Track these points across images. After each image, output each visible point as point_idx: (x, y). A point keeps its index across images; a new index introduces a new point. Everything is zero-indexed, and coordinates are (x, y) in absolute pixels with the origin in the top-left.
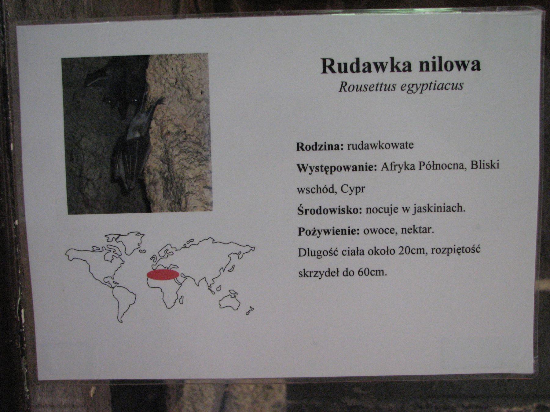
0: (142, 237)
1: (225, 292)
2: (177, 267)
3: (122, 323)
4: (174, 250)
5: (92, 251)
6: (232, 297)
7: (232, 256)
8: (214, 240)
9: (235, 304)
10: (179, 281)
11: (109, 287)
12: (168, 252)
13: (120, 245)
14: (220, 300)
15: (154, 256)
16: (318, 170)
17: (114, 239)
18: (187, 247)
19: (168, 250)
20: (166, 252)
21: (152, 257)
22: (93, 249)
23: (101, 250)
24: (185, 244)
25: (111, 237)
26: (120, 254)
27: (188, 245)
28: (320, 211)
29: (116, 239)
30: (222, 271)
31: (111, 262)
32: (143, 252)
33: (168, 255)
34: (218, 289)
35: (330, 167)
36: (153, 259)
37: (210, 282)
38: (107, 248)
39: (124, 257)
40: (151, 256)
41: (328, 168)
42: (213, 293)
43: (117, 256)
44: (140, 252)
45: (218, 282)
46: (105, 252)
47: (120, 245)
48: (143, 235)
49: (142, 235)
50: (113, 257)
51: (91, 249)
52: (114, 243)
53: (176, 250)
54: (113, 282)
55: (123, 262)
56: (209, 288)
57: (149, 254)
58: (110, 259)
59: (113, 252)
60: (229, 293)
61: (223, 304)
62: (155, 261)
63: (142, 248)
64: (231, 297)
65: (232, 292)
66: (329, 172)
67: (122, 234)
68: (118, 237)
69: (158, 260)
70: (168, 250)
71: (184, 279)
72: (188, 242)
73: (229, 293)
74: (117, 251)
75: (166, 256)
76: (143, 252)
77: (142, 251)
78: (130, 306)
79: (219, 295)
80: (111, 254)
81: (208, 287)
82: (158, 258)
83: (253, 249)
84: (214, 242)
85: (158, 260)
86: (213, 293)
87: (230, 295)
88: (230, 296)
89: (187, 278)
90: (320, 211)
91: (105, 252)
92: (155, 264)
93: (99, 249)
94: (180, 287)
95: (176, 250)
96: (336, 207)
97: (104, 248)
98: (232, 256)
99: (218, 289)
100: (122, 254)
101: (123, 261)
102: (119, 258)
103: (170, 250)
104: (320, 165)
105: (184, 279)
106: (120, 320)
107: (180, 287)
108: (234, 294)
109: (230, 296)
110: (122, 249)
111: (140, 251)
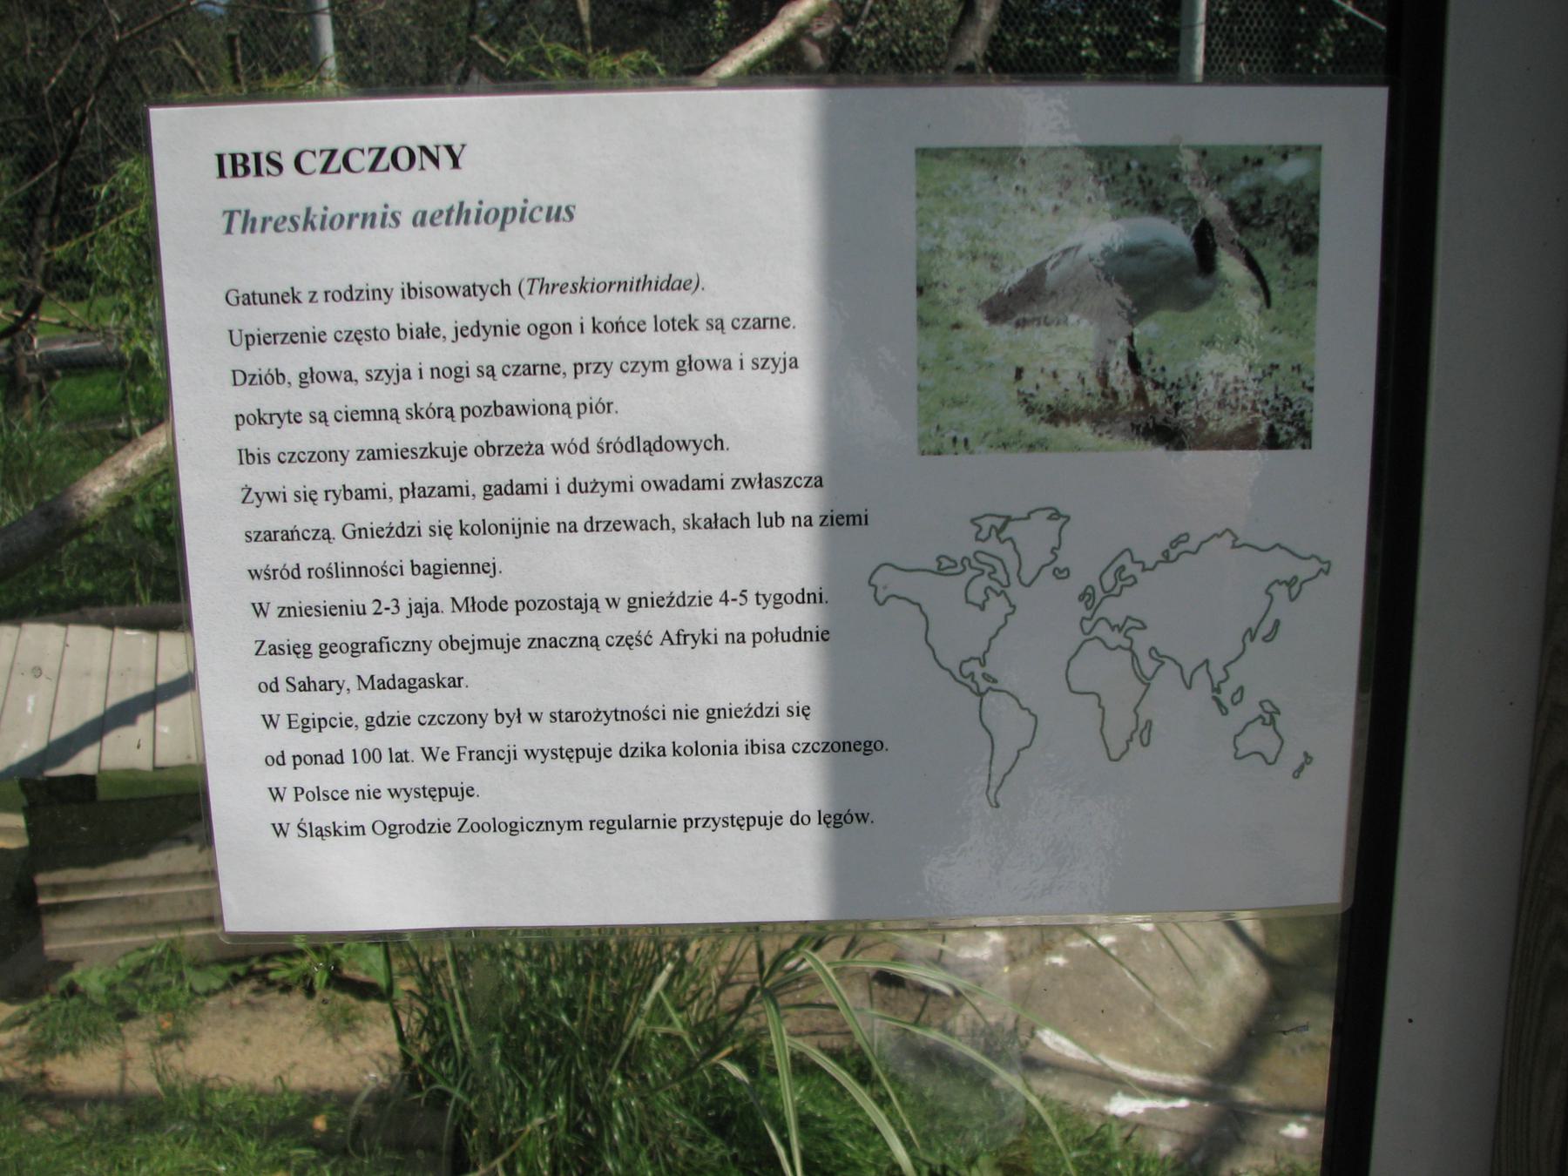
1: (1249, 709)
5: (935, 569)
9: (1269, 744)
13: (1006, 551)
14: (1238, 731)
15: (1090, 591)
22: (940, 563)
23: (960, 568)
26: (1005, 583)
31: (982, 607)
32: (1062, 574)
34: (1237, 698)
37: (1218, 675)
38: (974, 563)
39: (1015, 591)
43: (998, 588)
46: (970, 573)
47: (1006, 551)
52: (992, 546)
57: (1075, 585)
58: (979, 599)
60: (1259, 711)
61: (1246, 744)
62: (1089, 604)
65: (1268, 707)
73: (1259, 711)
74: (1000, 575)
75: (1116, 591)
76: (1062, 574)
79: (1239, 715)
80: (984, 581)
82: (1099, 594)
86: (1224, 710)
87: (1261, 717)
89: (1163, 663)
91: (970, 573)
97: (966, 562)
101: (1011, 605)
102: (1002, 596)
108: (1271, 714)
110: (1012, 565)
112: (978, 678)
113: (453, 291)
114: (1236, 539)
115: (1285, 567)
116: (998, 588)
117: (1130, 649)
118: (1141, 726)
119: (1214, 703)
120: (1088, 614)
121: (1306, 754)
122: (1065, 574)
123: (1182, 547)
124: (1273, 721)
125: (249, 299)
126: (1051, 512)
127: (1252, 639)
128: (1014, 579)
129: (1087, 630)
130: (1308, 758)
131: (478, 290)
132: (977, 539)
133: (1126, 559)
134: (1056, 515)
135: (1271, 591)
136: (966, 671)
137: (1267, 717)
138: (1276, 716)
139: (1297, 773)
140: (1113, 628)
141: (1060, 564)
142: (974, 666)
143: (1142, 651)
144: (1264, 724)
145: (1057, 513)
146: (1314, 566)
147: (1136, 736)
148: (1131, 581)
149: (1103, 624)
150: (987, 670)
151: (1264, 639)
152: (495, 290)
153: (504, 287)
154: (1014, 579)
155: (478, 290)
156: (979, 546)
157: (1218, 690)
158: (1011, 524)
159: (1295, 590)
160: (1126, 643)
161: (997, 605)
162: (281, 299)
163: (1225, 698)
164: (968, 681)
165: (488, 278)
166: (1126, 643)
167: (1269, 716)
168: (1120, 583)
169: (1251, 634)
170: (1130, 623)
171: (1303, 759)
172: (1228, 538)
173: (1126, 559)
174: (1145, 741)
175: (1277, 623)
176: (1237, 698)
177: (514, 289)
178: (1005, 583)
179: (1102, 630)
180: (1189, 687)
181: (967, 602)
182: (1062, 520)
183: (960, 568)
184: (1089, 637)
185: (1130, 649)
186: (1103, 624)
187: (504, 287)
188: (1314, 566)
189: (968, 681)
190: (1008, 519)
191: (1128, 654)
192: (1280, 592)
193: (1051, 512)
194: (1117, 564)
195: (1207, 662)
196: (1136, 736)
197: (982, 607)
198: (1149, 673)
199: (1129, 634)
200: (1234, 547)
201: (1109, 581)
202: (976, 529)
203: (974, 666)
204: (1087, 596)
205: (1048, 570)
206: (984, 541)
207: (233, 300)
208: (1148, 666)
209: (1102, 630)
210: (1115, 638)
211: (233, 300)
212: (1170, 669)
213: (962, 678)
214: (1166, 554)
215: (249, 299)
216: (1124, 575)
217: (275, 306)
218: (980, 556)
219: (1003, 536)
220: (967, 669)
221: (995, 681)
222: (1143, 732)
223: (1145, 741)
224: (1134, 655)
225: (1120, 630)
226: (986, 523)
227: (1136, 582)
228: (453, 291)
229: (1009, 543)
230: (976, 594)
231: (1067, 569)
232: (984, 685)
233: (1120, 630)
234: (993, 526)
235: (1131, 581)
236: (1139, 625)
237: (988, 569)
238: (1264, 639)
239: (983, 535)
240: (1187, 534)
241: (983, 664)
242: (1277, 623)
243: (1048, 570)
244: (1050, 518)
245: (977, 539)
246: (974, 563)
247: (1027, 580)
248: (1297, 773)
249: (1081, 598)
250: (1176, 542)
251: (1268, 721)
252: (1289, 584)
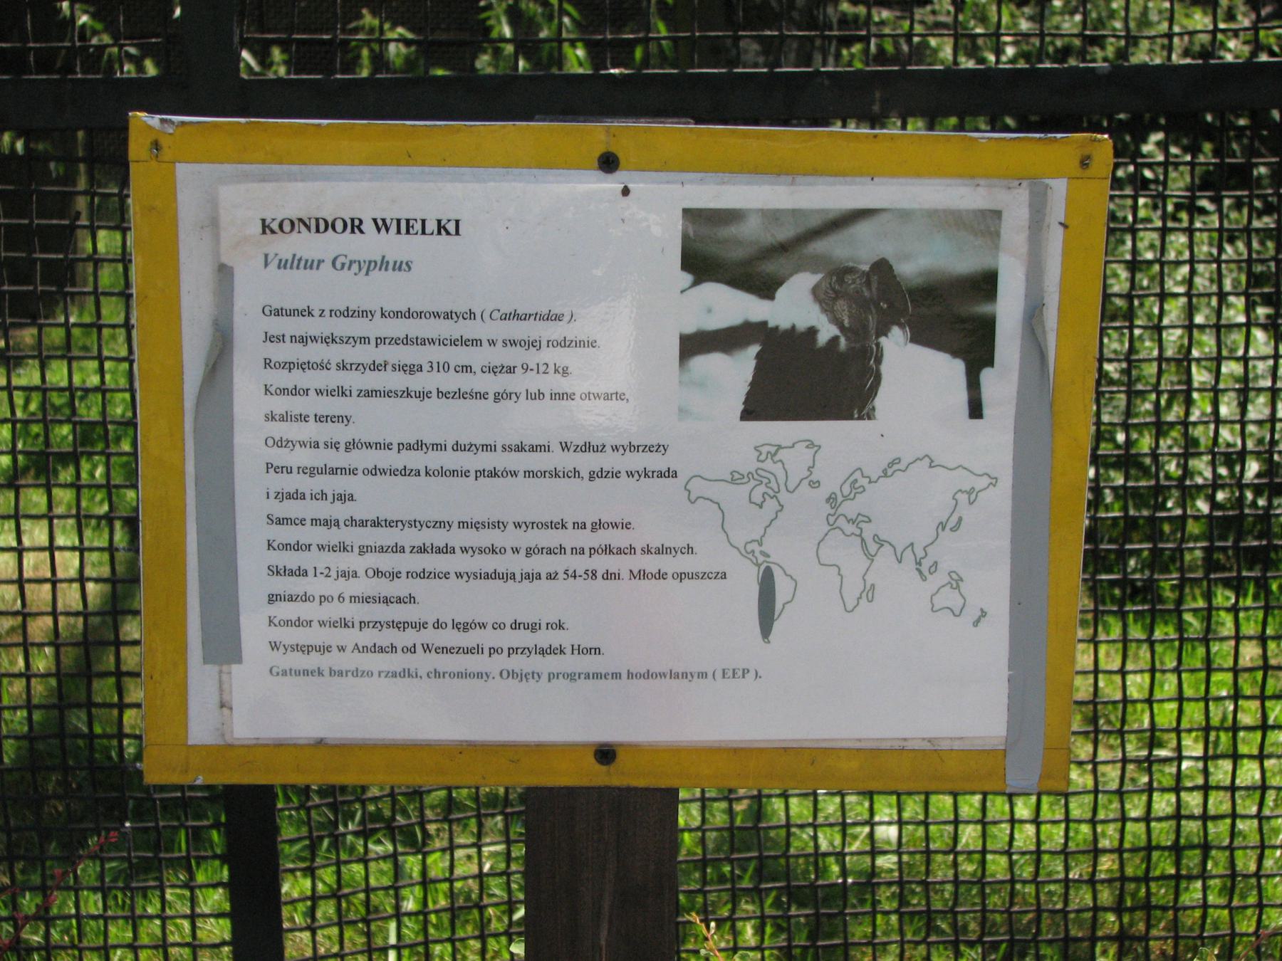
1: (940, 578)
9: (956, 602)
13: (777, 469)
31: (761, 507)
32: (815, 484)
34: (933, 569)
37: (920, 554)
38: (756, 476)
39: (783, 496)
40: (827, 496)
43: (772, 493)
46: (753, 483)
52: (768, 465)
57: (824, 492)
60: (947, 579)
61: (939, 601)
65: (954, 576)
68: (775, 454)
73: (947, 579)
74: (774, 485)
75: (852, 496)
76: (815, 484)
80: (762, 489)
82: (840, 499)
89: (882, 545)
91: (753, 483)
110: (782, 481)
112: (757, 554)
113: (436, 315)
114: (932, 461)
115: (967, 482)
116: (772, 493)
117: (860, 535)
118: (868, 587)
119: (917, 573)
120: (832, 512)
121: (982, 610)
123: (896, 467)
124: (958, 587)
125: (278, 312)
126: (808, 443)
127: (943, 529)
128: (783, 488)
129: (831, 522)
130: (984, 613)
131: (454, 315)
132: (758, 461)
133: (858, 475)
134: (811, 444)
135: (957, 497)
136: (749, 550)
138: (960, 583)
139: (976, 623)
140: (848, 522)
141: (814, 478)
143: (868, 535)
144: (952, 587)
145: (813, 444)
146: (985, 481)
147: (864, 595)
148: (861, 489)
149: (842, 518)
150: (763, 548)
151: (951, 529)
152: (465, 316)
153: (472, 315)
154: (783, 488)
155: (454, 315)
157: (919, 564)
158: (781, 451)
159: (973, 497)
160: (858, 532)
161: (771, 505)
162: (301, 313)
163: (925, 568)
164: (750, 556)
165: (462, 308)
166: (858, 532)
167: (956, 582)
168: (854, 491)
169: (942, 526)
170: (860, 518)
171: (980, 613)
172: (927, 460)
173: (858, 475)
175: (960, 519)
176: (933, 569)
177: (478, 316)
179: (842, 522)
180: (900, 562)
181: (751, 502)
183: (746, 480)
184: (833, 526)
185: (860, 535)
186: (842, 518)
187: (472, 315)
188: (985, 481)
189: (750, 556)
190: (780, 447)
191: (859, 540)
192: (963, 498)
193: (808, 443)
194: (852, 479)
195: (912, 544)
196: (864, 595)
197: (761, 507)
199: (860, 525)
200: (931, 467)
201: (846, 489)
202: (757, 454)
203: (754, 546)
204: (831, 499)
205: (806, 482)
206: (763, 461)
207: (267, 312)
208: (873, 548)
209: (842, 522)
210: (850, 528)
211: (267, 312)
212: (887, 548)
214: (885, 471)
215: (278, 312)
216: (857, 485)
217: (296, 318)
218: (760, 472)
219: (776, 458)
220: (750, 547)
221: (768, 556)
222: (869, 592)
224: (863, 540)
226: (764, 450)
228: (436, 315)
229: (780, 464)
230: (757, 497)
231: (818, 482)
234: (768, 453)
235: (861, 489)
236: (866, 519)
237: (765, 481)
238: (951, 529)
239: (762, 457)
240: (899, 459)
241: (761, 544)
242: (960, 519)
243: (806, 482)
245: (758, 461)
246: (756, 476)
247: (791, 488)
248: (976, 623)
249: (828, 500)
250: (891, 464)
251: (955, 586)
252: (969, 493)
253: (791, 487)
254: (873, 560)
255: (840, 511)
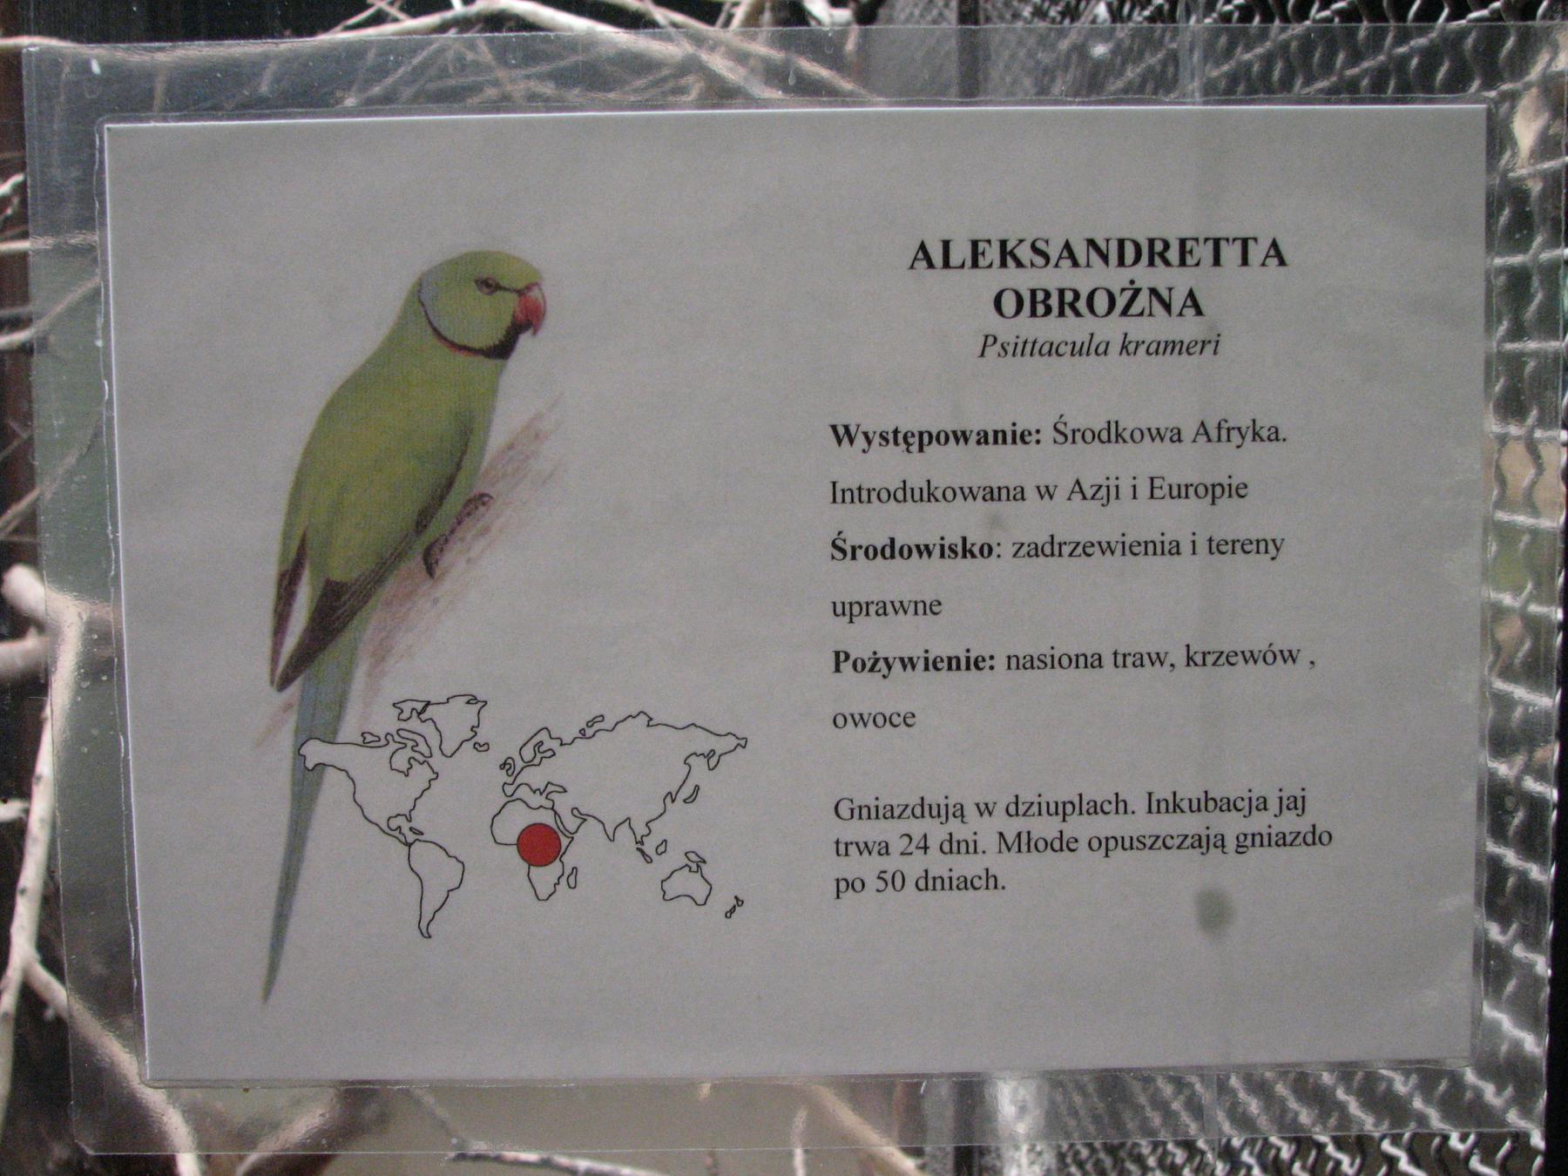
0: (481, 708)
1: (675, 858)
2: (561, 790)
3: (429, 940)
4: (555, 745)
6: (693, 869)
7: (692, 761)
8: (651, 719)
9: (700, 891)
10: (567, 827)
11: (400, 841)
12: (541, 750)
13: (428, 729)
14: (664, 878)
15: (510, 761)
16: (887, 441)
17: (415, 713)
18: (587, 736)
19: (541, 743)
20: (536, 749)
21: (505, 764)
22: (365, 738)
23: (383, 742)
24: (583, 729)
25: (407, 707)
26: (427, 754)
27: (589, 732)
28: (891, 550)
29: (419, 714)
30: (669, 800)
33: (542, 758)
34: (662, 849)
35: (917, 435)
36: (507, 767)
37: (641, 830)
38: (397, 738)
39: (437, 761)
41: (913, 435)
42: (648, 859)
43: (421, 759)
44: (477, 749)
45: (660, 830)
46: (393, 746)
47: (428, 729)
48: (483, 704)
49: (480, 704)
50: (412, 761)
51: (360, 740)
52: (414, 724)
53: (561, 744)
54: (411, 829)
55: (434, 776)
56: (639, 846)
58: (405, 767)
59: (412, 747)
61: (673, 887)
62: (510, 772)
63: (480, 739)
64: (690, 871)
66: (915, 448)
67: (433, 701)
69: (518, 769)
70: (541, 743)
71: (579, 821)
72: (590, 724)
73: (686, 861)
74: (423, 748)
75: (537, 761)
77: (481, 746)
78: (450, 893)
79: (663, 865)
80: (408, 753)
81: (637, 843)
82: (519, 764)
83: (743, 742)
84: (651, 723)
85: (518, 769)
87: (686, 865)
88: (687, 869)
89: (585, 820)
90: (891, 550)
91: (393, 746)
92: (510, 780)
93: (379, 741)
94: (570, 843)
95: (561, 744)
96: (932, 539)
97: (389, 737)
98: (692, 761)
99: (662, 849)
100: (434, 755)
103: (548, 744)
104: (891, 430)
105: (579, 821)
106: (424, 931)
107: (570, 843)
108: (697, 863)
109: (687, 869)
110: (434, 743)
111: (477, 746)
116: (421, 759)
117: (552, 809)
118: (568, 872)
122: (486, 747)
123: (597, 726)
128: (436, 751)
133: (543, 736)
134: (472, 700)
137: (694, 867)
138: (701, 864)
140: (534, 792)
142: (401, 821)
147: (563, 880)
148: (549, 753)
154: (436, 751)
156: (403, 725)
158: (430, 708)
160: (549, 804)
161: (421, 774)
163: (649, 848)
167: (697, 864)
170: (550, 788)
173: (543, 736)
174: (572, 885)
175: (697, 788)
178: (427, 754)
179: (524, 792)
182: (480, 704)
190: (428, 703)
194: (534, 741)
198: (572, 828)
199: (551, 796)
201: (528, 753)
205: (468, 746)
213: (392, 831)
216: (542, 749)
218: (401, 733)
219: (423, 717)
220: (394, 823)
223: (572, 885)
224: (556, 813)
225: (541, 794)
226: (407, 707)
227: (554, 754)
232: (411, 837)
233: (541, 794)
235: (549, 753)
236: (560, 789)
237: (410, 744)
239: (405, 716)
242: (697, 788)
243: (468, 746)
244: (468, 702)
247: (448, 750)
249: (503, 766)
253: (448, 750)
254: (573, 838)
255: (518, 781)
